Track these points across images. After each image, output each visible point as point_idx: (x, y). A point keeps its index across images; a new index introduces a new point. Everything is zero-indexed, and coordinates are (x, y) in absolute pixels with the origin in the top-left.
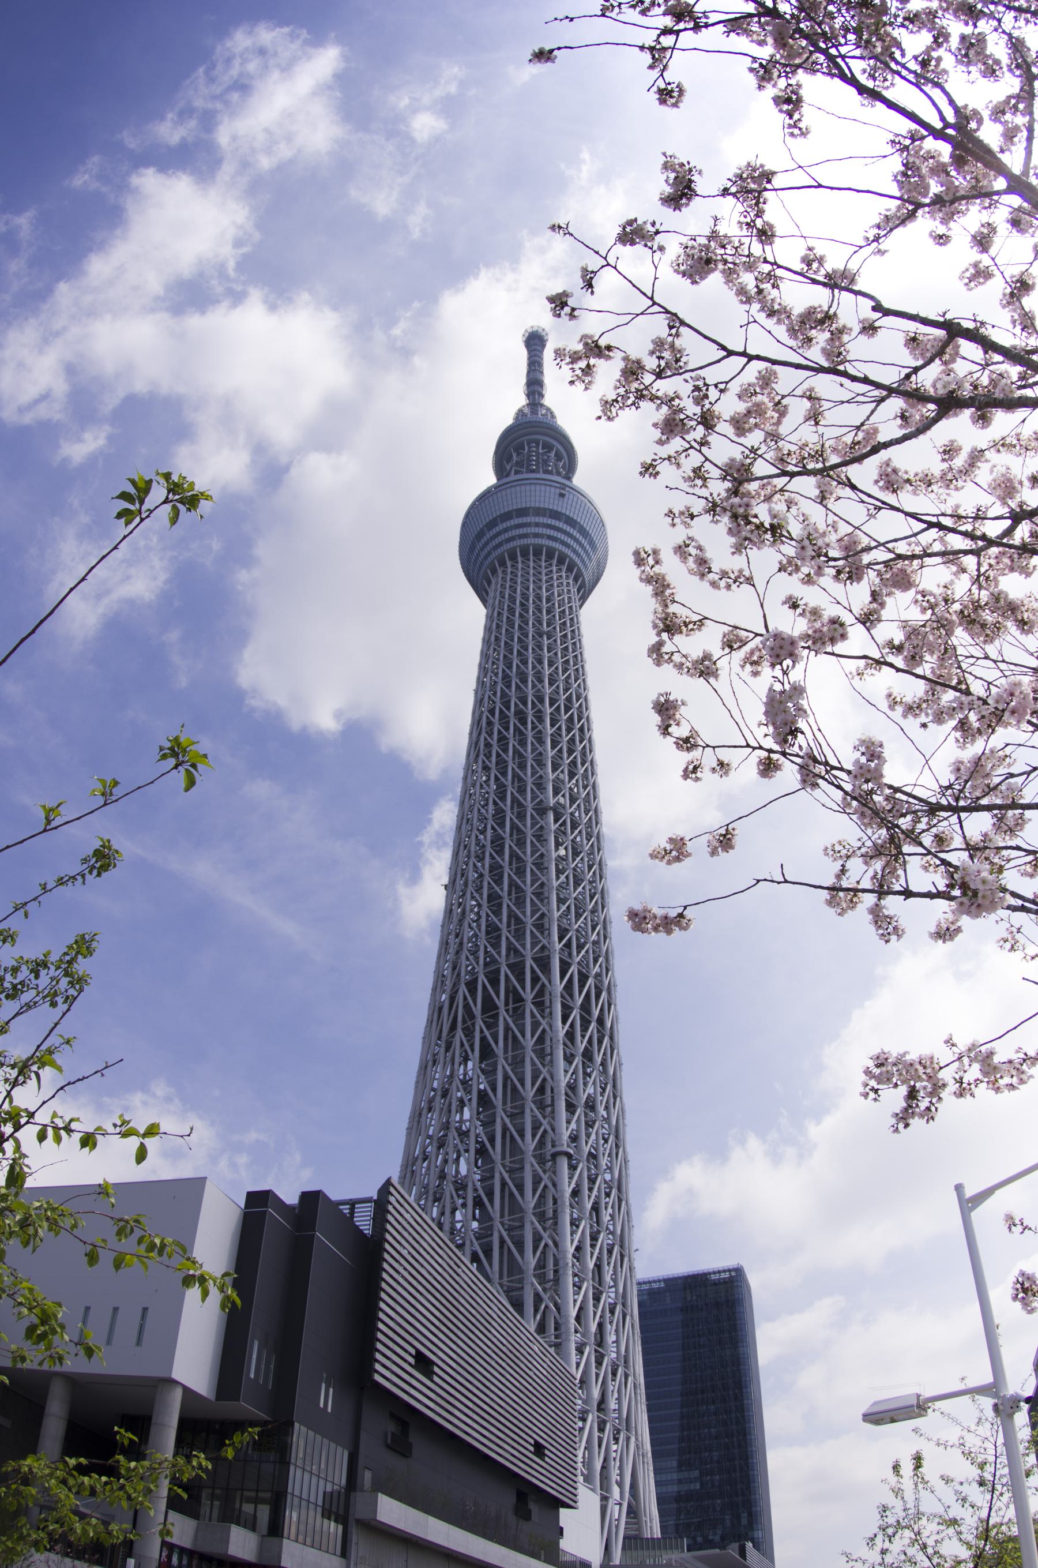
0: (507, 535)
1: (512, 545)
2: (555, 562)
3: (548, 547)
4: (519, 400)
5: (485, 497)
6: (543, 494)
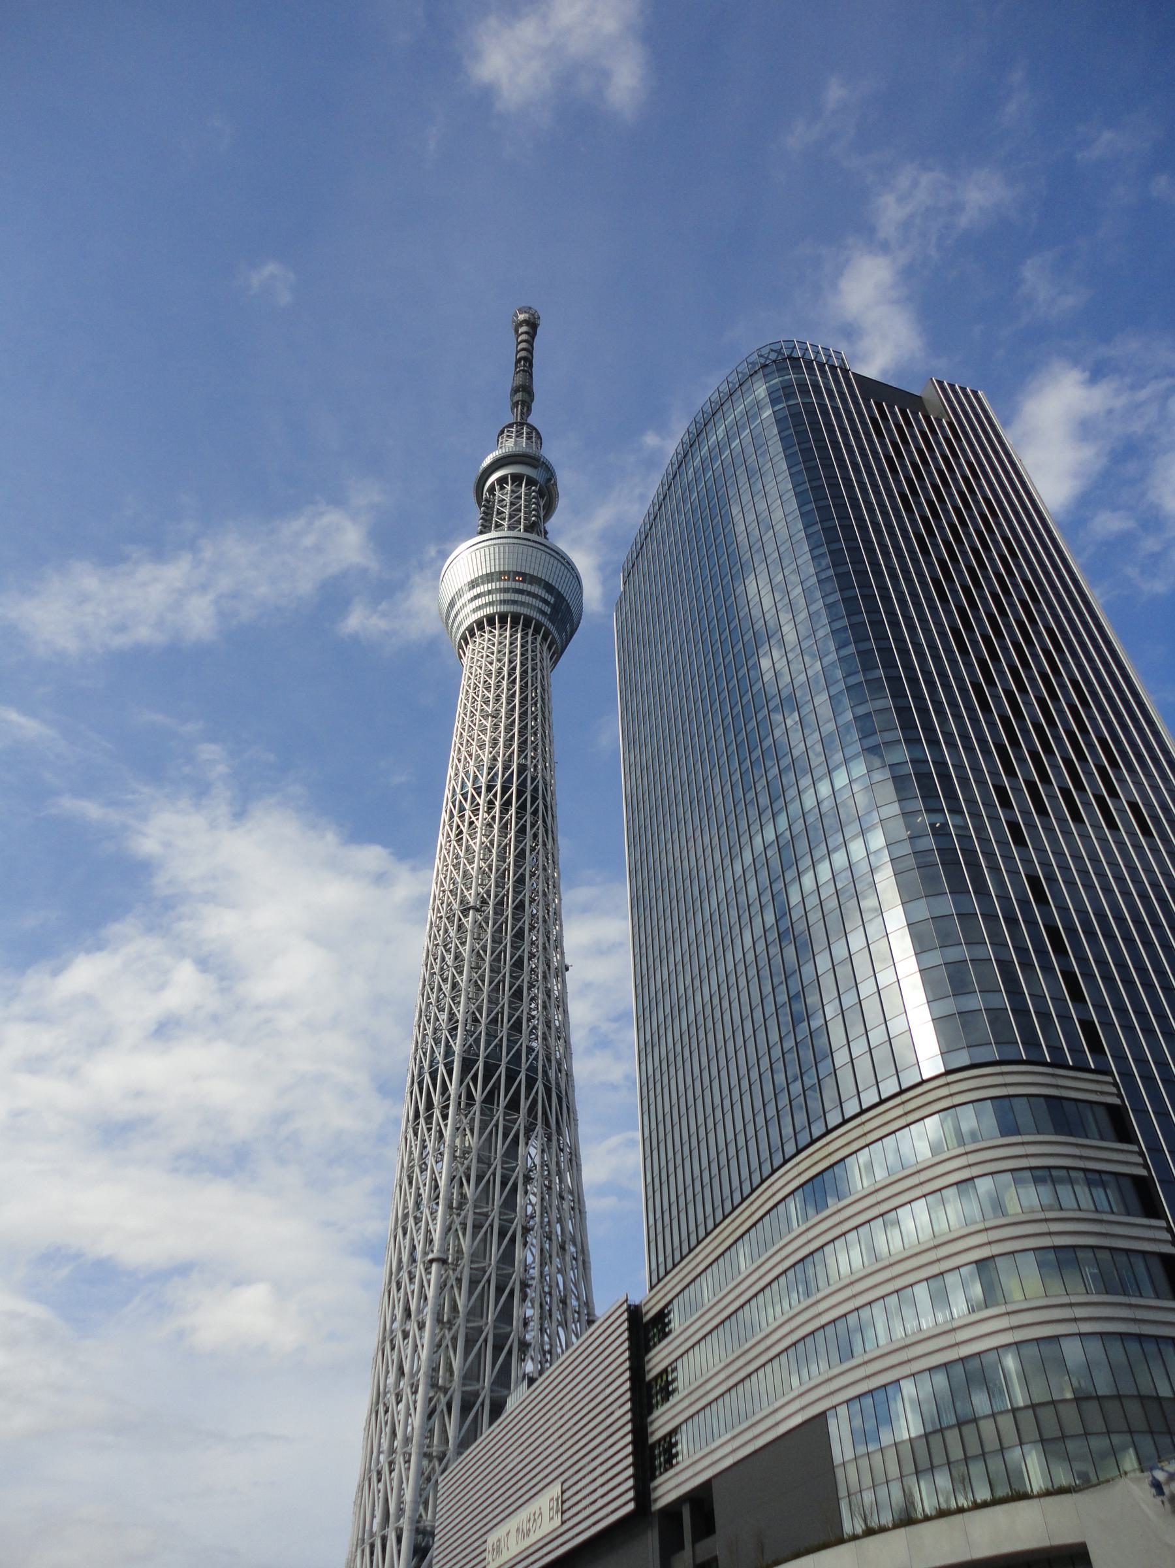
2: (531, 631)
3: (525, 616)
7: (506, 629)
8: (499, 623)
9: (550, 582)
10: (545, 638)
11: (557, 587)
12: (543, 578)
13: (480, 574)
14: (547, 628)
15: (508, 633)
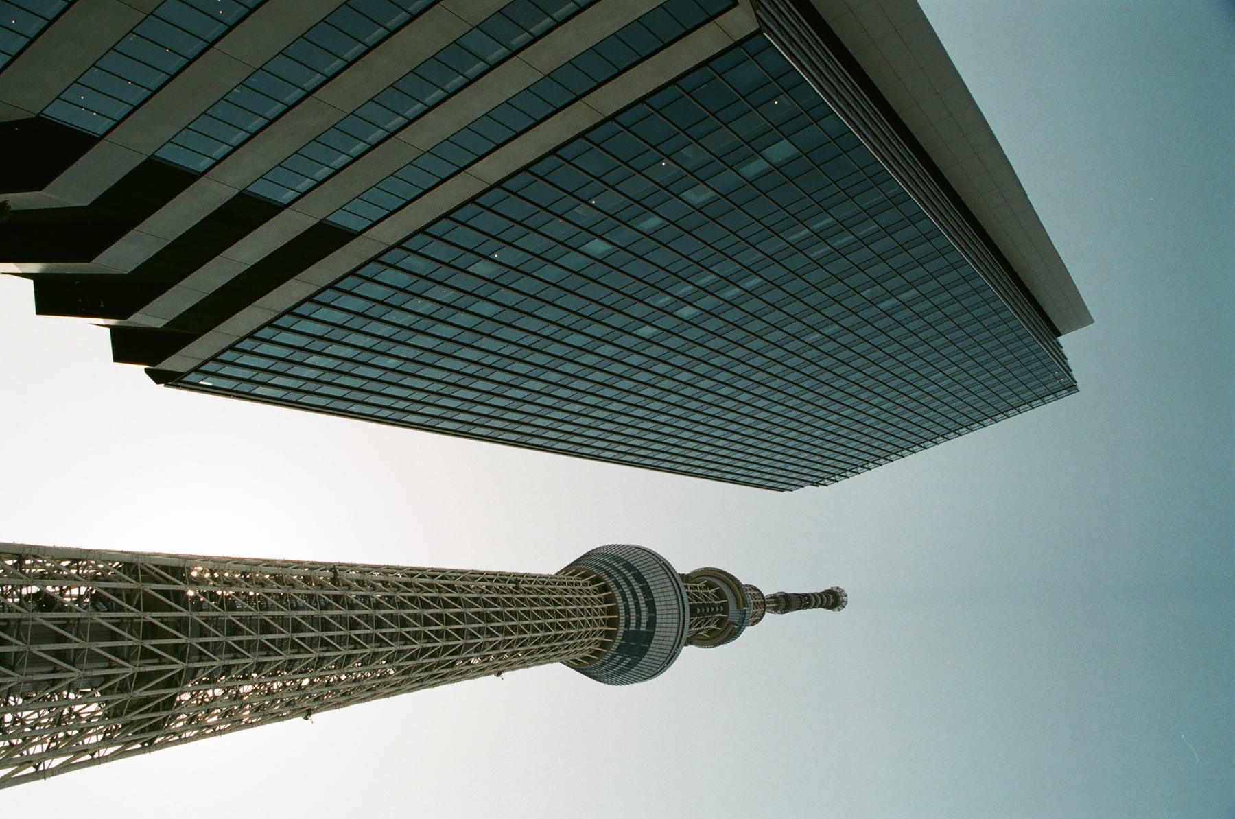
0: (628, 593)
1: (619, 598)
3: (616, 632)
4: (768, 590)
5: (666, 567)
6: (670, 621)
7: (603, 615)
8: (608, 607)
9: (648, 653)
10: (596, 653)
11: (644, 659)
12: (652, 645)
13: (650, 584)
14: (605, 653)
15: (600, 617)
